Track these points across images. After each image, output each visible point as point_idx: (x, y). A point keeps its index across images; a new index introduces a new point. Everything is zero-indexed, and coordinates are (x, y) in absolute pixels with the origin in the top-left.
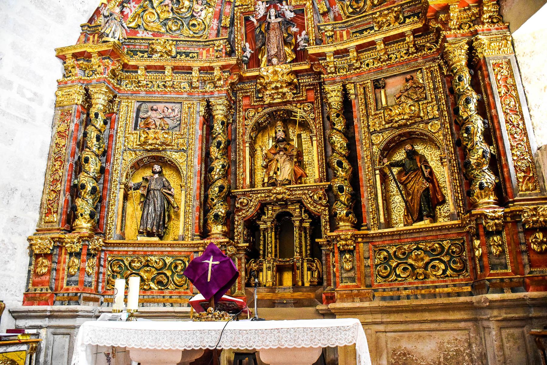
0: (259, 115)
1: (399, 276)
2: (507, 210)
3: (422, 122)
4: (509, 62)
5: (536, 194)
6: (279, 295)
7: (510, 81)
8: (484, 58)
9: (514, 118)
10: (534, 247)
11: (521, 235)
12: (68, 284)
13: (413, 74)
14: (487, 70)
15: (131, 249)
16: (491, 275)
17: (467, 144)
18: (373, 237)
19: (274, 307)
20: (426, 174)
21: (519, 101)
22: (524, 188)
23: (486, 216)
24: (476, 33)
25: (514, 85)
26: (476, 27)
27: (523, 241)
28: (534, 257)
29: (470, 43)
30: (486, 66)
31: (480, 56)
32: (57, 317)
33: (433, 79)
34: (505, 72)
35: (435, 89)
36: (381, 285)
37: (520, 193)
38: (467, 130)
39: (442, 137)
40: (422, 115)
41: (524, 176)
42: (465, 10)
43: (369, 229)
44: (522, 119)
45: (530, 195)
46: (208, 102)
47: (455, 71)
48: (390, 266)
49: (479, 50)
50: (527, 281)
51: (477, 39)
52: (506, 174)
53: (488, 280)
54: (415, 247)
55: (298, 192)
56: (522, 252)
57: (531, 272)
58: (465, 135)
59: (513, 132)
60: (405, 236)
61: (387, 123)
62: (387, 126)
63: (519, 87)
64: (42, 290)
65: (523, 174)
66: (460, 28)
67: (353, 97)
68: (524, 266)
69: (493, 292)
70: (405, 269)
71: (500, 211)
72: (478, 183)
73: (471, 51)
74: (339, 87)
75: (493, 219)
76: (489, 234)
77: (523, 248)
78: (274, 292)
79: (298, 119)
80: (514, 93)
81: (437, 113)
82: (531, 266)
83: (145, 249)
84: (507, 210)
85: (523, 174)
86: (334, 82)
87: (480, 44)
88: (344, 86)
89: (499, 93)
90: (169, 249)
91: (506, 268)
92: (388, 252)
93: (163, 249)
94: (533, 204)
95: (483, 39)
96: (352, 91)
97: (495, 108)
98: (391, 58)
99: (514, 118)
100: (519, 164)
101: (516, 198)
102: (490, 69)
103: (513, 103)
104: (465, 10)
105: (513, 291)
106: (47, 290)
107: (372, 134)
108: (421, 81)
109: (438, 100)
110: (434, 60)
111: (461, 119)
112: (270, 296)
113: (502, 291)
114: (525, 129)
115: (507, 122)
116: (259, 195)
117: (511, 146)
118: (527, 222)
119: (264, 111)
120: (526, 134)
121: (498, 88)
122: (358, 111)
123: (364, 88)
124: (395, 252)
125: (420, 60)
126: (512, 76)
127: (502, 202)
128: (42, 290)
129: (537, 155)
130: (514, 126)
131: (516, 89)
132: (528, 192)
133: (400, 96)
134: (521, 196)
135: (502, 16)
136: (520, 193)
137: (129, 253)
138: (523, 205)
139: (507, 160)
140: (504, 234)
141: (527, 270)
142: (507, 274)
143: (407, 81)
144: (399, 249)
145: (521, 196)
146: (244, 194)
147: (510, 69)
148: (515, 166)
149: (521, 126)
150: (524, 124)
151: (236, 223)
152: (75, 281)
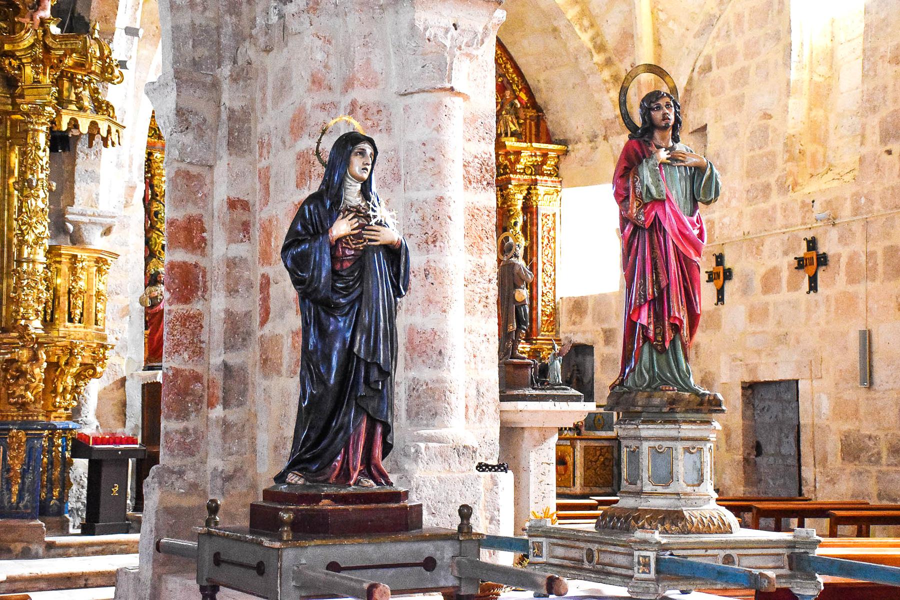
2: (533, 347)
4: (554, 215)
7: (552, 233)
9: (549, 269)
22: (545, 330)
24: (535, 182)
26: (538, 177)
29: (529, 189)
30: (537, 214)
31: (534, 203)
37: (542, 333)
41: (547, 320)
42: (531, 156)
45: (548, 336)
47: (512, 213)
49: (534, 198)
51: (535, 189)
65: (546, 318)
66: (524, 173)
73: (527, 198)
80: (552, 246)
84: (533, 347)
85: (546, 318)
87: (537, 194)
95: (541, 189)
99: (549, 269)
100: (545, 309)
101: (539, 337)
103: (550, 255)
104: (531, 156)
115: (543, 271)
117: (543, 293)
120: (554, 284)
126: (554, 229)
129: (559, 304)
132: (547, 333)
134: (542, 335)
135: (558, 168)
136: (542, 333)
138: (543, 344)
145: (542, 335)
147: (554, 222)
148: (542, 311)
149: (552, 277)
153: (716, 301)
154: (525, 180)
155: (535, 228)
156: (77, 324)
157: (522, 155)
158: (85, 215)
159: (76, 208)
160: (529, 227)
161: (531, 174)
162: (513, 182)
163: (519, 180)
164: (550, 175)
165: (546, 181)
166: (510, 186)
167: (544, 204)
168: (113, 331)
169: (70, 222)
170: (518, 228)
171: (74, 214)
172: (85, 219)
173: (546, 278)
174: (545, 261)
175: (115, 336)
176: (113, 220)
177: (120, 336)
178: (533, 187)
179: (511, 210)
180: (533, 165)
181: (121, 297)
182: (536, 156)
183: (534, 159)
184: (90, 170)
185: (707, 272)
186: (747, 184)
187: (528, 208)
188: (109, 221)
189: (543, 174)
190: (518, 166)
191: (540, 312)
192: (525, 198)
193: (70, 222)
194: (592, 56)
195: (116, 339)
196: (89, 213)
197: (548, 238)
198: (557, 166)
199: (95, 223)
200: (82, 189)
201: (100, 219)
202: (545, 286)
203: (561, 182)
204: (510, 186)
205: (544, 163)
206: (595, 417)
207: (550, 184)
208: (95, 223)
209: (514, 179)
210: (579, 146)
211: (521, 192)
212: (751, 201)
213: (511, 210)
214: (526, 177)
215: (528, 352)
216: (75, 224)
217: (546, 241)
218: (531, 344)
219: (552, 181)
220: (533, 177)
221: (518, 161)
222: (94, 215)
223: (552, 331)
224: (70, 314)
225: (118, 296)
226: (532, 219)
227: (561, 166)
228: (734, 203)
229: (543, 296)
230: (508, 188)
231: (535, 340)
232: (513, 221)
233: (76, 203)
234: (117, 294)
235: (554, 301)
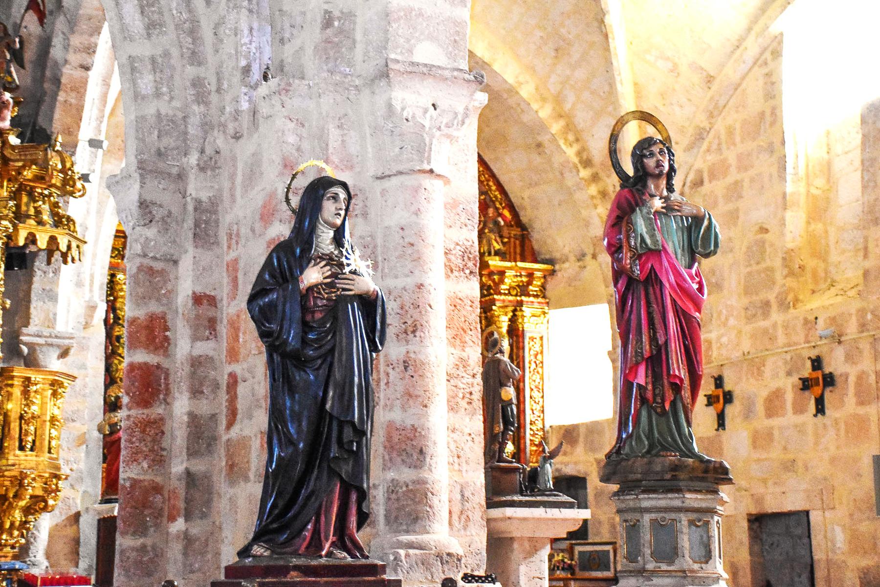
4: (541, 338)
7: (539, 357)
14: (523, 342)
24: (520, 304)
26: (523, 298)
29: (514, 311)
30: (523, 338)
31: (520, 326)
41: (536, 450)
49: (520, 320)
51: (521, 310)
52: (522, 446)
59: (534, 408)
66: (509, 294)
73: (513, 320)
85: (534, 448)
95: (527, 311)
99: (536, 395)
102: (527, 341)
115: (531, 398)
120: (543, 412)
121: (530, 363)
126: (542, 353)
130: (535, 402)
135: (545, 289)
139: (525, 433)
147: (542, 345)
149: (541, 404)
153: (716, 427)
154: (510, 301)
155: (521, 351)
157: (507, 274)
159: (32, 329)
161: (516, 295)
162: (498, 304)
163: (504, 301)
164: (536, 296)
165: (533, 302)
166: (494, 308)
167: (530, 325)
168: (68, 461)
169: (26, 344)
171: (29, 335)
173: (534, 405)
174: (533, 387)
175: (70, 466)
176: (71, 341)
177: (75, 467)
178: (518, 308)
180: (518, 286)
181: (77, 425)
182: (521, 276)
183: (519, 279)
184: (48, 288)
185: (705, 396)
186: (745, 301)
187: (515, 333)
188: (67, 342)
189: (529, 295)
190: (503, 287)
191: (528, 442)
192: (510, 320)
194: (578, 171)
195: (71, 470)
196: (45, 334)
197: (535, 362)
198: (543, 287)
199: (51, 345)
200: (39, 308)
203: (548, 303)
204: (494, 308)
205: (529, 283)
206: (590, 557)
207: (536, 305)
208: (51, 345)
209: (498, 300)
210: (567, 265)
212: (750, 319)
214: (511, 298)
216: (32, 347)
217: (533, 366)
220: (519, 298)
221: (502, 281)
222: (50, 336)
224: (21, 440)
225: (74, 424)
226: (518, 342)
227: (548, 287)
228: (732, 322)
229: (531, 424)
230: (492, 310)
233: (31, 324)
234: (73, 421)
235: (543, 429)
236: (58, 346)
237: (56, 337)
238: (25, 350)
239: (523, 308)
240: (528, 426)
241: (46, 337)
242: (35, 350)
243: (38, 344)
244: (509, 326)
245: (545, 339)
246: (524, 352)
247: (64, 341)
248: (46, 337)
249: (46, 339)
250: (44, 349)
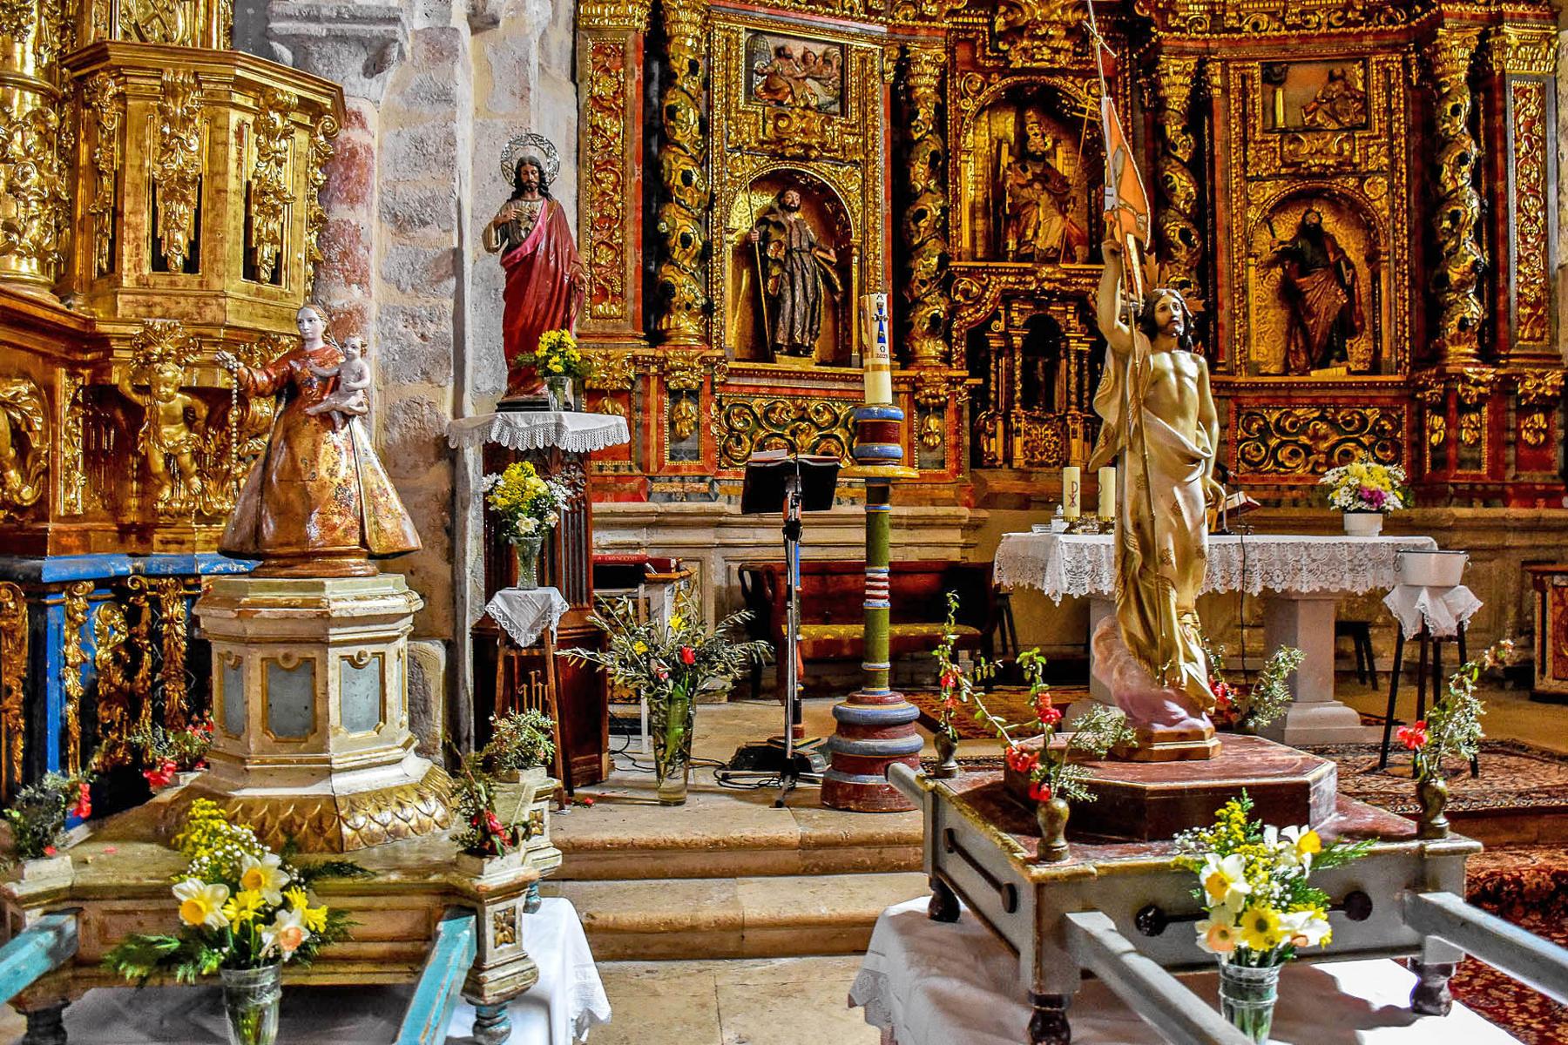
0: (992, 89)
1: (1282, 465)
3: (1353, 174)
5: (1543, 348)
6: (1039, 487)
7: (1538, 128)
8: (1503, 71)
10: (1527, 436)
11: (1512, 415)
12: (672, 458)
13: (1347, 67)
14: (1504, 100)
15: (764, 382)
16: (1459, 477)
17: (1446, 242)
18: (1239, 388)
19: (1027, 508)
20: (1348, 279)
21: (1545, 172)
23: (1464, 379)
25: (1543, 139)
27: (1513, 426)
28: (1524, 453)
29: (1483, 36)
32: (667, 526)
33: (1389, 88)
34: (1533, 110)
35: (1389, 111)
36: (1246, 479)
38: (1454, 217)
39: (1386, 213)
40: (1356, 160)
41: (1530, 315)
43: (1231, 373)
44: (1545, 207)
46: (903, 50)
47: (1446, 90)
48: (1267, 446)
50: (1510, 490)
51: (1498, 33)
52: (1501, 307)
53: (1454, 485)
54: (1317, 414)
55: (1084, 281)
56: (1509, 443)
57: (1516, 477)
58: (1447, 224)
59: (1526, 231)
60: (1299, 393)
61: (1285, 165)
62: (1283, 171)
63: (1550, 145)
64: (617, 468)
65: (1528, 310)
67: (1217, 92)
68: (1507, 466)
69: (1459, 505)
70: (1295, 454)
71: (1489, 374)
72: (1457, 318)
74: (1191, 63)
75: (1477, 384)
76: (1464, 409)
77: (1512, 436)
78: (1028, 480)
79: (1086, 116)
81: (1386, 161)
82: (1517, 469)
83: (795, 384)
84: (1502, 372)
86: (1181, 53)
88: (1201, 63)
89: (1517, 150)
90: (842, 386)
91: (1479, 467)
92: (1264, 418)
93: (829, 385)
94: (1538, 366)
95: (1511, 33)
96: (1217, 80)
97: (1505, 177)
98: (1308, 22)
101: (1512, 352)
103: (1535, 175)
105: (1486, 505)
106: (630, 469)
107: (1251, 179)
108: (1360, 86)
109: (1392, 137)
110: (1394, 48)
111: (1440, 189)
112: (1019, 486)
113: (1470, 505)
114: (1545, 226)
115: (1519, 209)
116: (1004, 278)
117: (1520, 257)
118: (1526, 395)
119: (1004, 82)
121: (1517, 140)
122: (1225, 129)
123: (1244, 78)
124: (1278, 420)
125: (1368, 42)
126: (1543, 119)
127: (1487, 355)
128: (617, 468)
130: (1529, 219)
131: (1543, 148)
133: (1315, 110)
137: (763, 391)
139: (1508, 280)
140: (1485, 410)
141: (1511, 473)
142: (1479, 477)
143: (1332, 78)
144: (1288, 414)
145: (1523, 347)
146: (970, 272)
148: (1520, 295)
150: (1546, 218)
151: (955, 334)
152: (691, 452)
154: (1474, 17)
155: (1499, 118)
156: (182, 278)
158: (316, 19)
160: (1482, 121)
162: (1449, 23)
163: (1461, 16)
166: (1441, 31)
168: (413, 317)
169: (285, 39)
170: (1460, 122)
171: (289, 17)
172: (315, 29)
175: (420, 329)
176: (390, 28)
179: (1445, 84)
181: (433, 232)
187: (1485, 81)
188: (378, 29)
191: (1514, 297)
192: (1472, 56)
193: (285, 39)
195: (423, 336)
197: (1528, 139)
199: (342, 39)
201: (355, 26)
202: (1525, 242)
204: (1441, 31)
208: (342, 39)
209: (1450, 15)
211: (1464, 44)
213: (1445, 84)
215: (1489, 383)
218: (1497, 365)
219: (1537, 16)
220: (1494, 9)
222: (340, 18)
223: (1541, 339)
224: (156, 243)
225: (427, 230)
229: (1519, 262)
230: (1436, 37)
231: (1503, 357)
232: (1449, 106)
234: (424, 223)
236: (361, 42)
237: (354, 19)
238: (286, 54)
239: (1507, 29)
240: (1513, 267)
241: (329, 19)
242: (308, 54)
243: (310, 38)
244: (1470, 68)
245: (1550, 96)
246: (1505, 120)
247: (371, 27)
248: (329, 19)
249: (331, 26)
250: (328, 49)
